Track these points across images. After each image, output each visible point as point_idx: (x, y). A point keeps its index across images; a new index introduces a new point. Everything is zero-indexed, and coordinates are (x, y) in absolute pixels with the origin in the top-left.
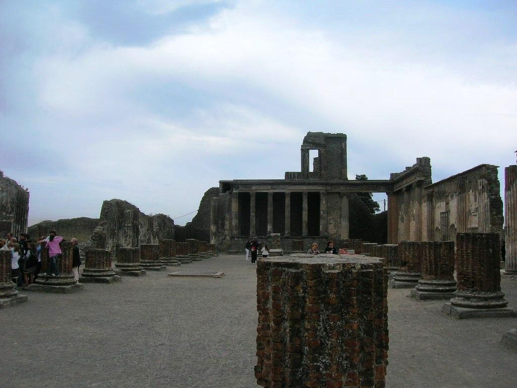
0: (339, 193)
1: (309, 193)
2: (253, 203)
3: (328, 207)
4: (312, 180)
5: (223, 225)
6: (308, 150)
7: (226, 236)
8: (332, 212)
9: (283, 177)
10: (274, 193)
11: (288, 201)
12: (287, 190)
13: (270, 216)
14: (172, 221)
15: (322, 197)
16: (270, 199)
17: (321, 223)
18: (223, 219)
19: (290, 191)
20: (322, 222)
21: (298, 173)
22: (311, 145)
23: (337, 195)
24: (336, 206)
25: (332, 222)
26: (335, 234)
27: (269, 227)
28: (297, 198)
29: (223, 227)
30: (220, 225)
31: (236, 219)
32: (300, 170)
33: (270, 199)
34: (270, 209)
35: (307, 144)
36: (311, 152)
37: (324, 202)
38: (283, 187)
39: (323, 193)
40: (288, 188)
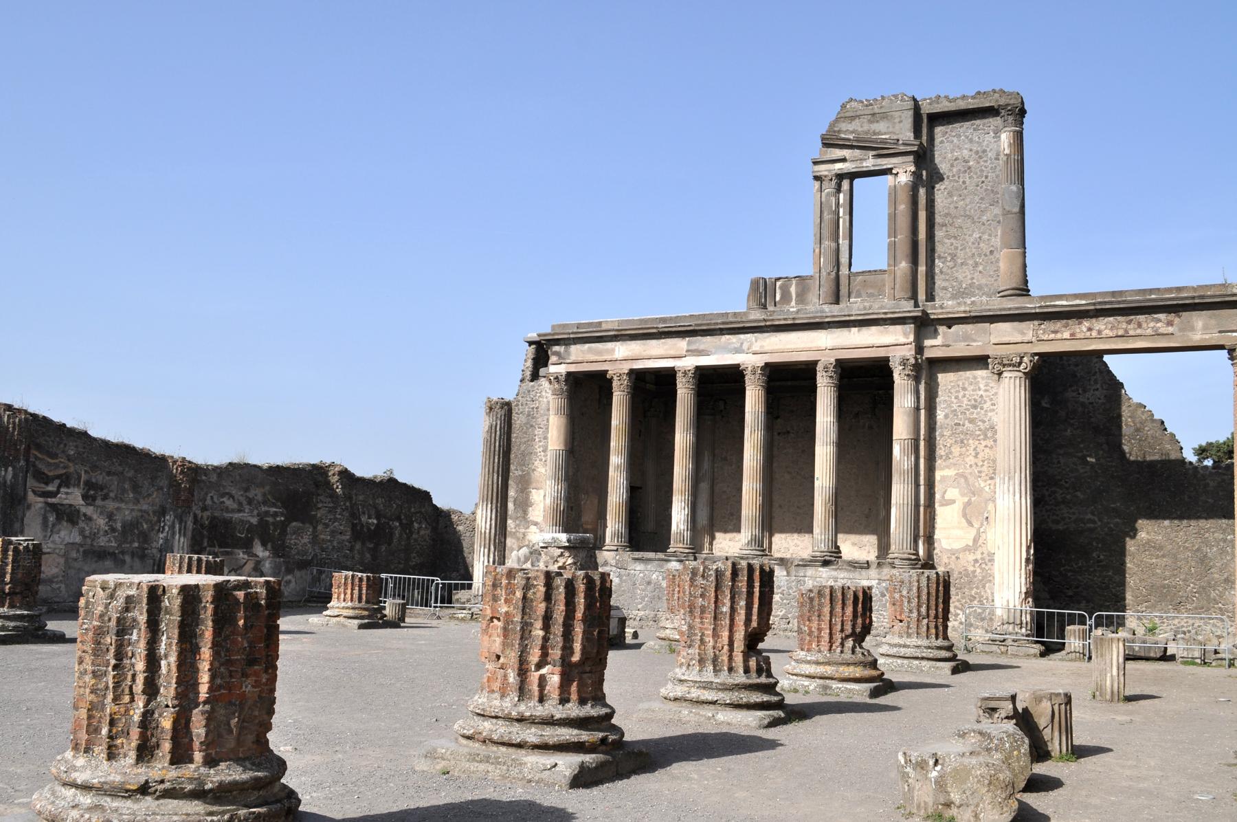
1: (839, 363)
4: (855, 306)
8: (956, 450)
10: (698, 368)
12: (750, 354)
14: (425, 496)
15: (896, 376)
16: (684, 395)
17: (893, 501)
19: (760, 361)
20: (900, 492)
22: (857, 152)
24: (972, 421)
25: (953, 493)
26: (967, 549)
29: (525, 512)
31: (557, 480)
32: (808, 269)
33: (684, 395)
34: (682, 439)
38: (734, 339)
39: (904, 362)
40: (756, 348)
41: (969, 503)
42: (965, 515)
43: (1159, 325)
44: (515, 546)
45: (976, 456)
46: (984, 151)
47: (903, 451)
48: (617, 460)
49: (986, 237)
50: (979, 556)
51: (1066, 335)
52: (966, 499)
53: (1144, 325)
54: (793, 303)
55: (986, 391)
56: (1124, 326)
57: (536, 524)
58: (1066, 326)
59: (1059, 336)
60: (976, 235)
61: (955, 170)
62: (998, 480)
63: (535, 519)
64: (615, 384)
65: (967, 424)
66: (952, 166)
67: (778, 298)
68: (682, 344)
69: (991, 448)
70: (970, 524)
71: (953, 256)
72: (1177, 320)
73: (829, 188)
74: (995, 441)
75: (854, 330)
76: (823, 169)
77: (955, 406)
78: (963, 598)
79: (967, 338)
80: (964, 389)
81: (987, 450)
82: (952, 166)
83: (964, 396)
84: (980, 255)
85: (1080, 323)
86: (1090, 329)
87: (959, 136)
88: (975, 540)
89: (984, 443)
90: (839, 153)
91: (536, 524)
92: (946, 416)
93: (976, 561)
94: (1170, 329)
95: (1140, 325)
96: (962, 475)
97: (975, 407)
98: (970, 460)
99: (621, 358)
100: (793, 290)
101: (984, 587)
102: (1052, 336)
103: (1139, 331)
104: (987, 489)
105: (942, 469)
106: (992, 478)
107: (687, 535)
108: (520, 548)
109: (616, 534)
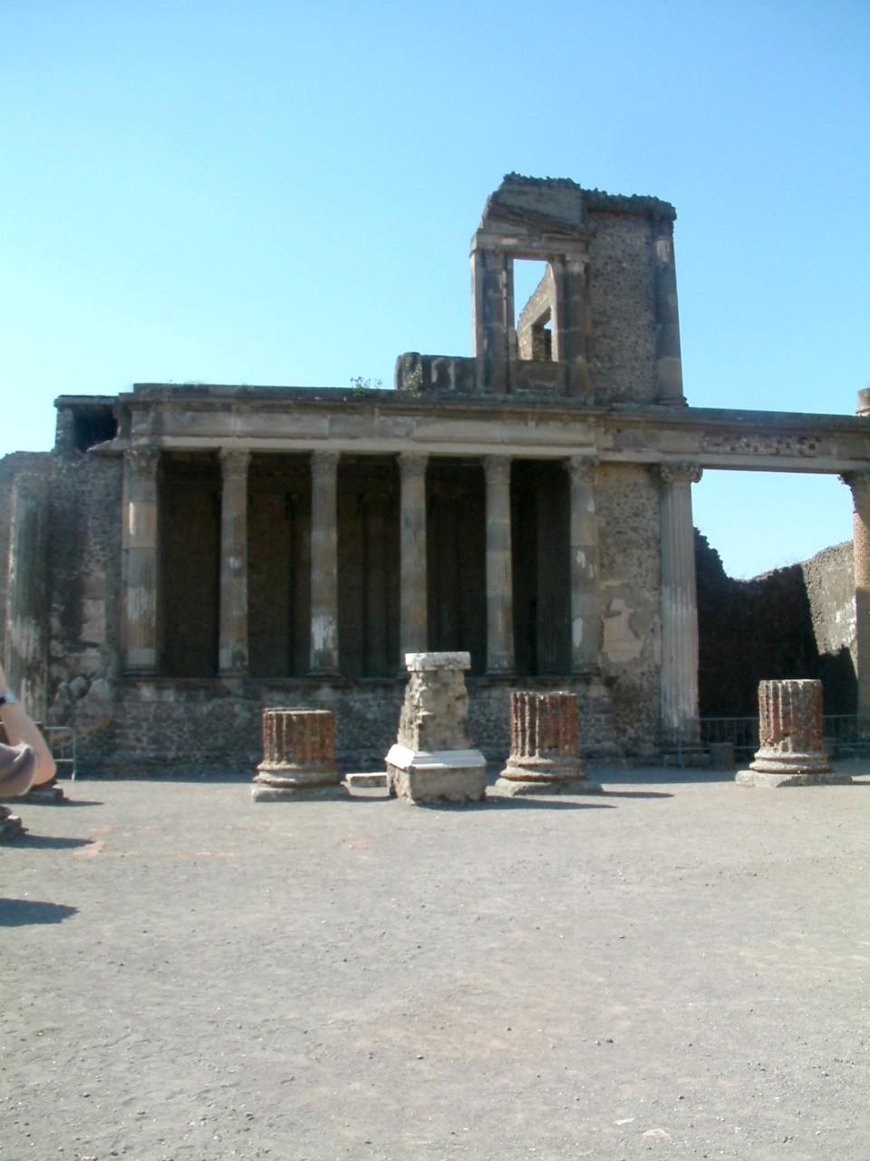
0: (652, 469)
2: (234, 506)
3: (602, 535)
5: (73, 619)
6: (509, 255)
7: (88, 678)
8: (619, 559)
9: (384, 378)
11: (413, 497)
13: (323, 574)
15: (577, 480)
16: (325, 482)
18: (74, 595)
20: (581, 603)
21: (462, 363)
22: (524, 231)
23: (641, 478)
24: (635, 529)
25: (618, 604)
26: (635, 662)
27: (322, 633)
28: (456, 482)
29: (78, 632)
30: (55, 623)
31: (149, 588)
33: (325, 482)
34: (323, 538)
35: (494, 225)
36: (519, 266)
37: (591, 507)
39: (586, 461)
40: (418, 432)
41: (632, 617)
42: (631, 627)
43: (804, 447)
44: (64, 675)
45: (641, 564)
46: (637, 255)
47: (588, 558)
48: (232, 562)
49: (641, 341)
50: (645, 669)
51: (728, 448)
52: (632, 611)
53: (792, 446)
54: (452, 387)
55: (648, 499)
56: (776, 445)
57: (94, 645)
58: (727, 440)
59: (721, 449)
60: (633, 338)
61: (609, 268)
62: (666, 591)
63: (93, 640)
64: (229, 465)
65: (629, 531)
66: (606, 264)
67: (434, 378)
68: (323, 423)
69: (655, 558)
70: (637, 635)
71: (610, 360)
72: (817, 445)
73: (494, 264)
74: (659, 551)
75: (532, 424)
76: (490, 241)
77: (617, 514)
78: (632, 711)
79: (637, 445)
80: (626, 496)
81: (650, 560)
82: (606, 264)
83: (626, 503)
84: (636, 359)
85: (739, 438)
86: (748, 445)
87: (611, 235)
88: (642, 653)
89: (647, 553)
90: (506, 227)
91: (94, 645)
92: (608, 524)
93: (643, 674)
94: (812, 452)
95: (788, 446)
96: (628, 586)
97: (636, 515)
98: (634, 570)
99: (236, 437)
100: (452, 371)
101: (651, 699)
102: (716, 448)
103: (788, 451)
104: (652, 600)
105: (606, 579)
106: (656, 589)
107: (335, 654)
108: (72, 677)
109: (237, 657)
